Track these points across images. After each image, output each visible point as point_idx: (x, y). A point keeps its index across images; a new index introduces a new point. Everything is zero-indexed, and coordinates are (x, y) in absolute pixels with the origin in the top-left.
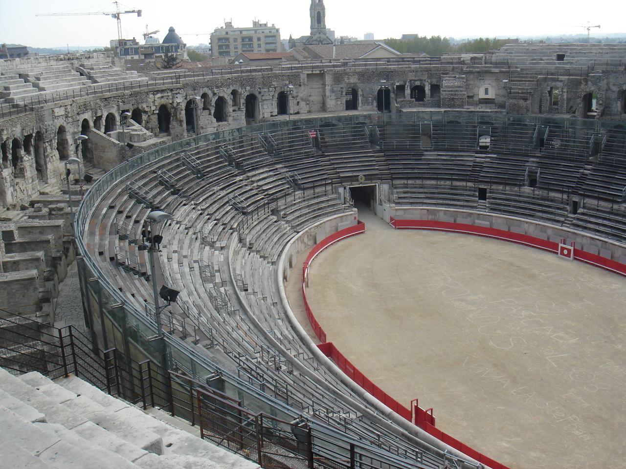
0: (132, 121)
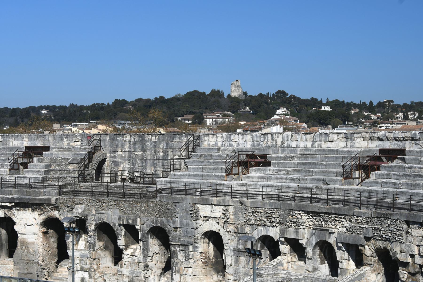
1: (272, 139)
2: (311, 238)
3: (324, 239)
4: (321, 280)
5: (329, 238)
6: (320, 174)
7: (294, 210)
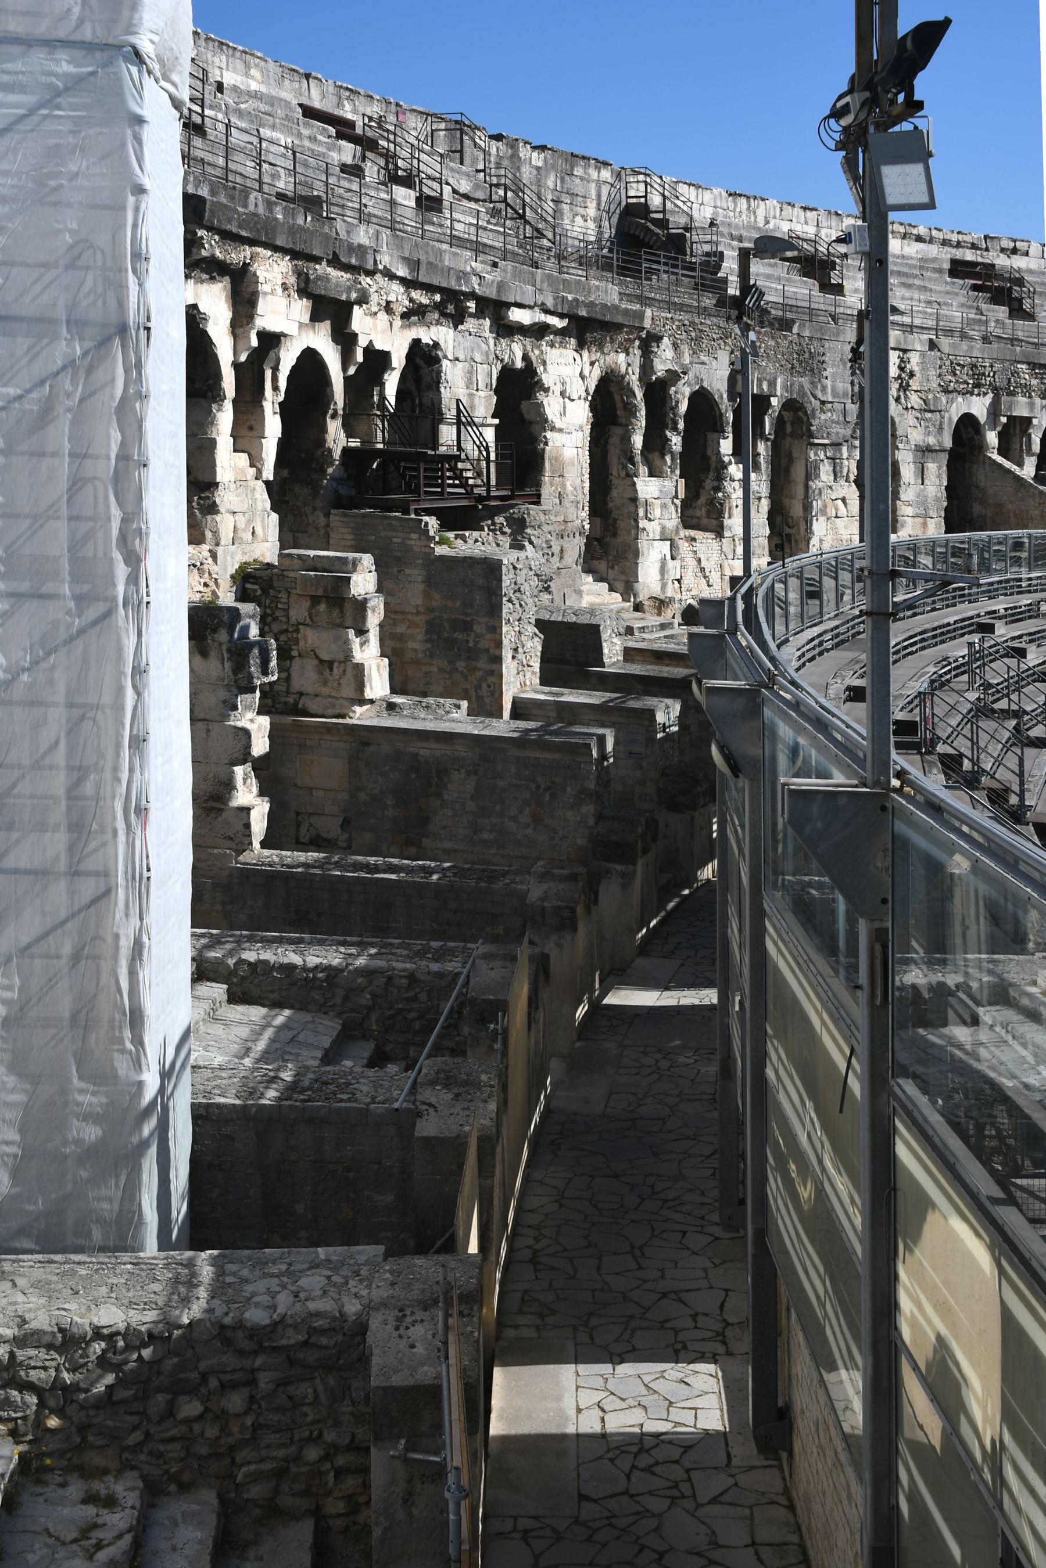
1: (748, 208)
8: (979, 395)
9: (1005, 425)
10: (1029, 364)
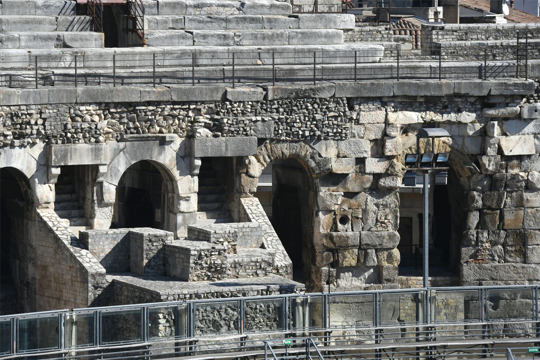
0: (252, 205)
2: (116, 160)
3: (148, 158)
4: (248, 230)
5: (160, 154)
6: (19, 25)
7: (76, 103)
8: (22, 146)
9: (60, 177)
10: (99, 104)
